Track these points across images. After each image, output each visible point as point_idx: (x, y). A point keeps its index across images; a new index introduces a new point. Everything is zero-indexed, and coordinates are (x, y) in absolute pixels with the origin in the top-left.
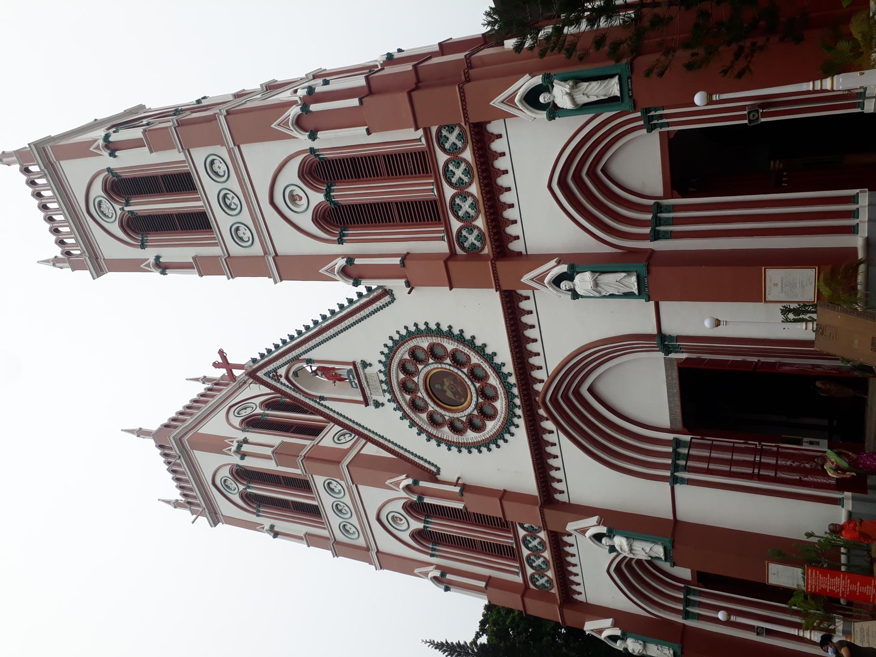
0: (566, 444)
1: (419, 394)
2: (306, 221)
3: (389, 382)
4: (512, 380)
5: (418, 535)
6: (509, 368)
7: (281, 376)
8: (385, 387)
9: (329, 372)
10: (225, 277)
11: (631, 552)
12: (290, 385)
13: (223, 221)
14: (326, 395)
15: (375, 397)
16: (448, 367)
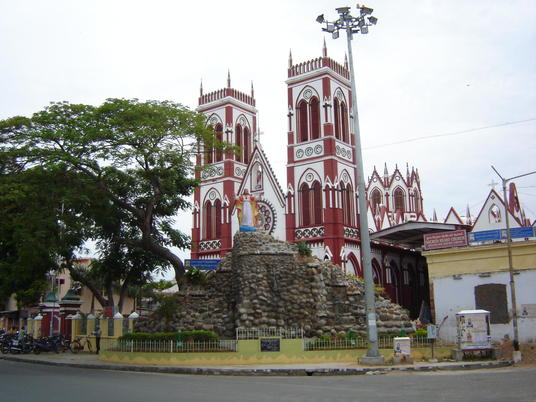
2: (303, 180)
5: (209, 203)
9: (260, 178)
10: (287, 144)
13: (304, 147)
14: (252, 176)
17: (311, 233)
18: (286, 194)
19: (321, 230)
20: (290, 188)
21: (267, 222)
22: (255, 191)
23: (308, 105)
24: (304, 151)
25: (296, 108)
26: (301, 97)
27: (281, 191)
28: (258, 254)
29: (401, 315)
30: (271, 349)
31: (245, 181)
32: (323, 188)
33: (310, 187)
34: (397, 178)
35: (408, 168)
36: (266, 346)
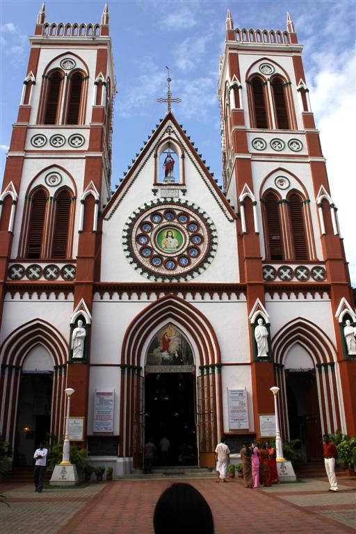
0: (143, 307)
1: (164, 220)
3: (172, 203)
4: (182, 280)
6: (190, 280)
7: (170, 134)
11: (76, 338)
12: (163, 138)
22: (166, 185)
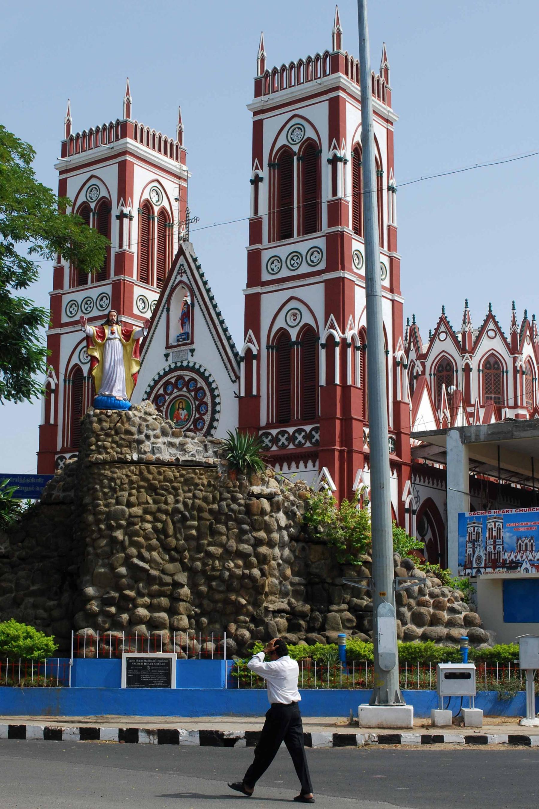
3: (182, 368)
7: (181, 276)
8: (179, 364)
12: (176, 283)
13: (283, 252)
15: (171, 354)
16: (194, 415)
17: (292, 439)
18: (241, 353)
19: (314, 433)
20: (250, 341)
21: (199, 413)
23: (295, 158)
24: (284, 259)
25: (270, 165)
26: (282, 141)
27: (232, 347)
28: (132, 462)
29: (464, 614)
30: (151, 682)
31: (155, 324)
32: (323, 340)
33: (294, 339)
34: (492, 334)
35: (514, 314)
36: (139, 676)
